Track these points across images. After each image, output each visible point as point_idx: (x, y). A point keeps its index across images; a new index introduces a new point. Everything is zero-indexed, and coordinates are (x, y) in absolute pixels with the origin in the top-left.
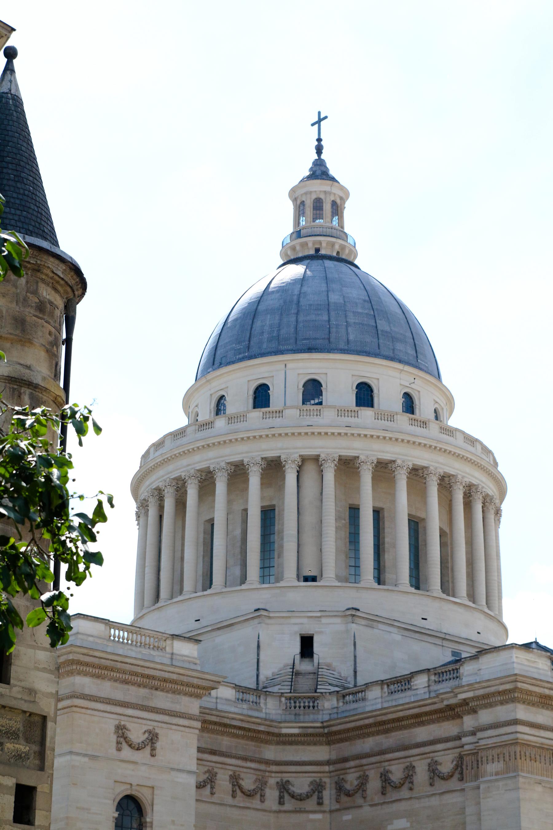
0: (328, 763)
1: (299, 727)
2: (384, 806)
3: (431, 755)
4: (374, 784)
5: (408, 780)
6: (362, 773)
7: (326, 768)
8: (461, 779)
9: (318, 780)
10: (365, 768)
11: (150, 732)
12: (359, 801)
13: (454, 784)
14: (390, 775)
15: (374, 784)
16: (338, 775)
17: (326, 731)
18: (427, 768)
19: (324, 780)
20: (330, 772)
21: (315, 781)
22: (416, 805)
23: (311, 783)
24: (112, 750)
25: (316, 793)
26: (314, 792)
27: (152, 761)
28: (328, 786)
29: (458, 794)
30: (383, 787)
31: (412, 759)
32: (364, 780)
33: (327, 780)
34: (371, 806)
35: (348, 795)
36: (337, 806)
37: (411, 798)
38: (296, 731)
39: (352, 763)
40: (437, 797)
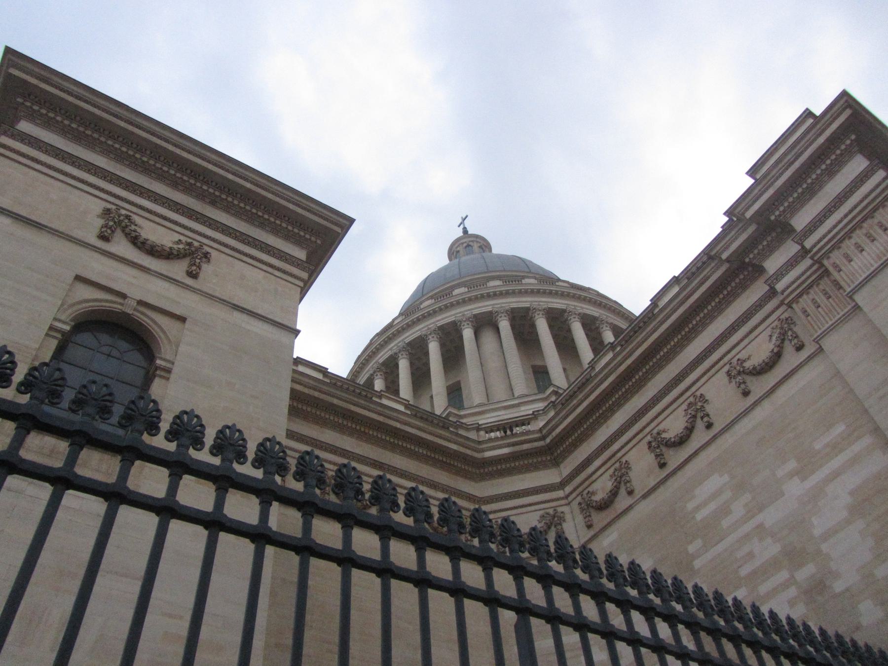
0: (562, 485)
1: (508, 445)
2: (669, 483)
3: (726, 359)
4: (641, 461)
5: (699, 415)
6: (617, 465)
7: (560, 493)
8: (799, 348)
9: (551, 511)
10: (619, 455)
11: (190, 244)
12: (623, 501)
13: (791, 359)
14: (664, 435)
15: (641, 461)
16: (581, 494)
17: (548, 440)
18: (726, 379)
19: (560, 509)
20: (567, 497)
21: (548, 514)
22: (728, 440)
23: (542, 517)
24: (94, 241)
25: (553, 528)
26: (549, 528)
27: (189, 281)
28: (568, 517)
29: (806, 369)
30: (657, 456)
31: (693, 389)
32: (621, 478)
33: (566, 509)
34: (645, 496)
35: (604, 506)
36: (592, 533)
37: (715, 438)
38: (506, 451)
39: (597, 463)
40: (766, 404)
